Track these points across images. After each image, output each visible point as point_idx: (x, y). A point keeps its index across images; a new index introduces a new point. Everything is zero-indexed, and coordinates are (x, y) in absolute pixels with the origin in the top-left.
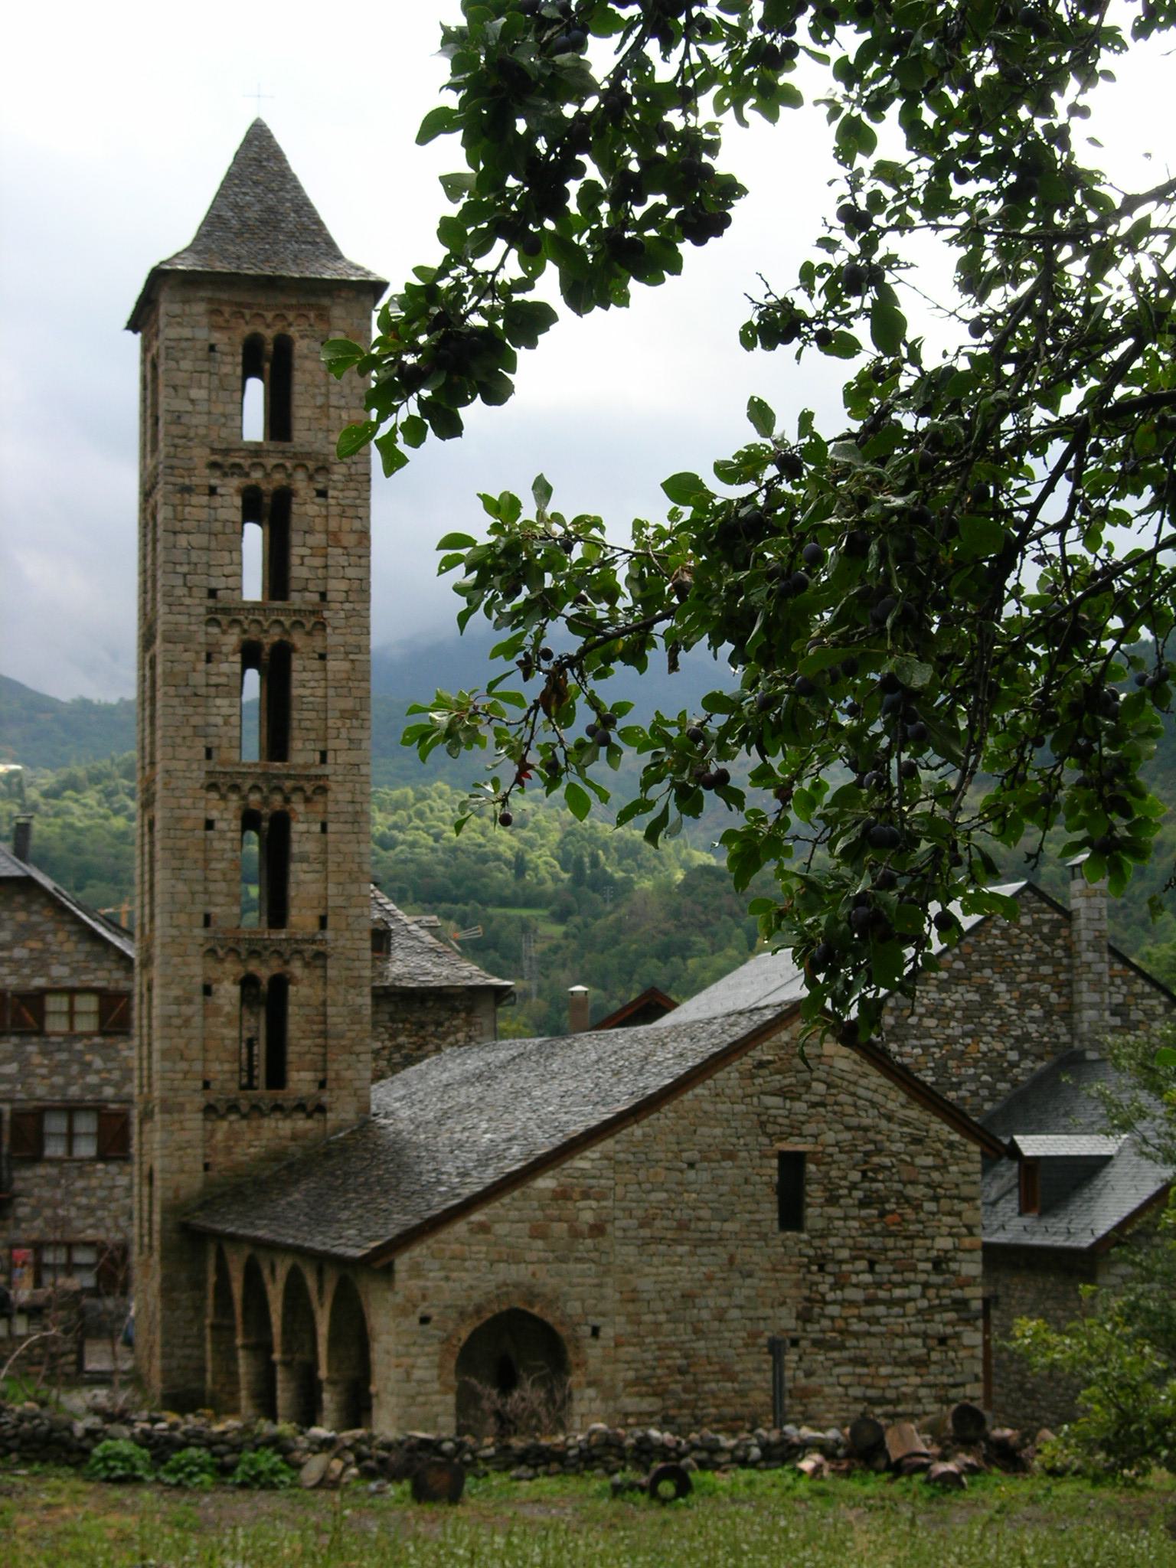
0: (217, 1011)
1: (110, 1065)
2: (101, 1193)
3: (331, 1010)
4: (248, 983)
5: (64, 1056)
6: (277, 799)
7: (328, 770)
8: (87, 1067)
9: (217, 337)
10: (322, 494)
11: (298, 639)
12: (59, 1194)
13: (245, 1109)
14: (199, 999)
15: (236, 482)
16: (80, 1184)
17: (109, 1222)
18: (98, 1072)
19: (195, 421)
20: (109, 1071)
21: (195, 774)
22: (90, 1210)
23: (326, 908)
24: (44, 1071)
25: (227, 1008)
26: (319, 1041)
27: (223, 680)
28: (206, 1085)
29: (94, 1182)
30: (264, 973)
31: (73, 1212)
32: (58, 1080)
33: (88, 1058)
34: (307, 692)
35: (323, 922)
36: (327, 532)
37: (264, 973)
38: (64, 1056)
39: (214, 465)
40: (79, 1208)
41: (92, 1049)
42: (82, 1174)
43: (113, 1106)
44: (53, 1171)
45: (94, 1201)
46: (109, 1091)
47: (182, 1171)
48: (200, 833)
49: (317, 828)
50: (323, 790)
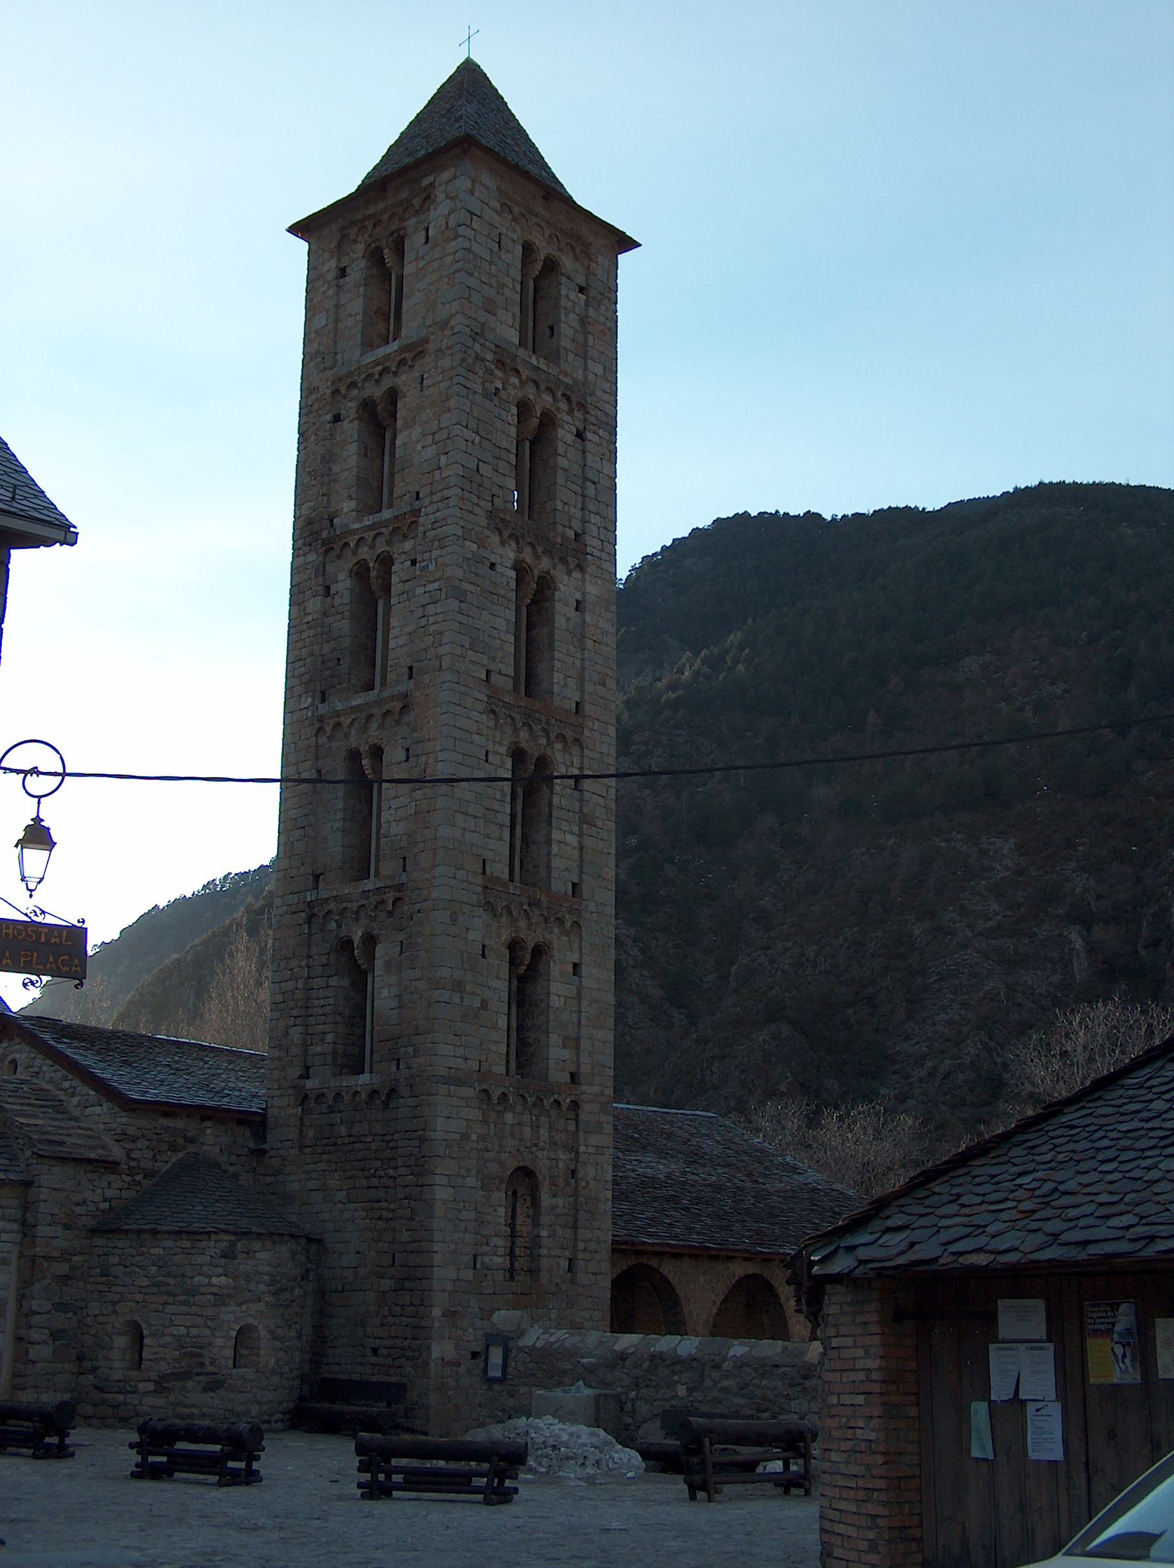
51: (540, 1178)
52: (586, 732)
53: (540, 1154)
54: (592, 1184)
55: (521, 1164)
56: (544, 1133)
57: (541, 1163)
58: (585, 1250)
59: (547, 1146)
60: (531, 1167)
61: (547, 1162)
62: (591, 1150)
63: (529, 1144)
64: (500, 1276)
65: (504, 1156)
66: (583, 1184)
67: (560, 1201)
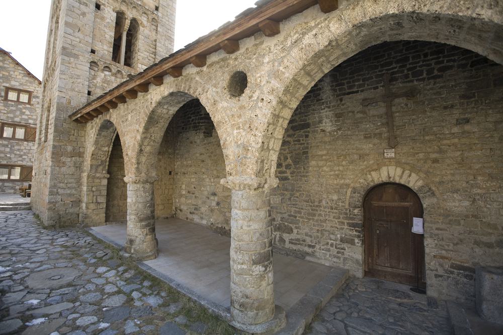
0: (103, 18)
1: (32, 114)
2: (25, 151)
3: (158, 44)
5: (14, 108)
8: (23, 113)
12: (8, 150)
13: (114, 71)
16: (16, 147)
17: (27, 160)
18: (27, 115)
20: (32, 116)
22: (21, 156)
24: (5, 112)
25: (108, 20)
26: (153, 56)
28: (93, 52)
29: (22, 148)
31: (13, 156)
32: (11, 115)
33: (24, 110)
35: (157, 8)
38: (14, 108)
40: (16, 154)
41: (25, 108)
42: (18, 144)
43: (31, 126)
44: (5, 142)
45: (22, 153)
46: (31, 121)
47: (73, 90)
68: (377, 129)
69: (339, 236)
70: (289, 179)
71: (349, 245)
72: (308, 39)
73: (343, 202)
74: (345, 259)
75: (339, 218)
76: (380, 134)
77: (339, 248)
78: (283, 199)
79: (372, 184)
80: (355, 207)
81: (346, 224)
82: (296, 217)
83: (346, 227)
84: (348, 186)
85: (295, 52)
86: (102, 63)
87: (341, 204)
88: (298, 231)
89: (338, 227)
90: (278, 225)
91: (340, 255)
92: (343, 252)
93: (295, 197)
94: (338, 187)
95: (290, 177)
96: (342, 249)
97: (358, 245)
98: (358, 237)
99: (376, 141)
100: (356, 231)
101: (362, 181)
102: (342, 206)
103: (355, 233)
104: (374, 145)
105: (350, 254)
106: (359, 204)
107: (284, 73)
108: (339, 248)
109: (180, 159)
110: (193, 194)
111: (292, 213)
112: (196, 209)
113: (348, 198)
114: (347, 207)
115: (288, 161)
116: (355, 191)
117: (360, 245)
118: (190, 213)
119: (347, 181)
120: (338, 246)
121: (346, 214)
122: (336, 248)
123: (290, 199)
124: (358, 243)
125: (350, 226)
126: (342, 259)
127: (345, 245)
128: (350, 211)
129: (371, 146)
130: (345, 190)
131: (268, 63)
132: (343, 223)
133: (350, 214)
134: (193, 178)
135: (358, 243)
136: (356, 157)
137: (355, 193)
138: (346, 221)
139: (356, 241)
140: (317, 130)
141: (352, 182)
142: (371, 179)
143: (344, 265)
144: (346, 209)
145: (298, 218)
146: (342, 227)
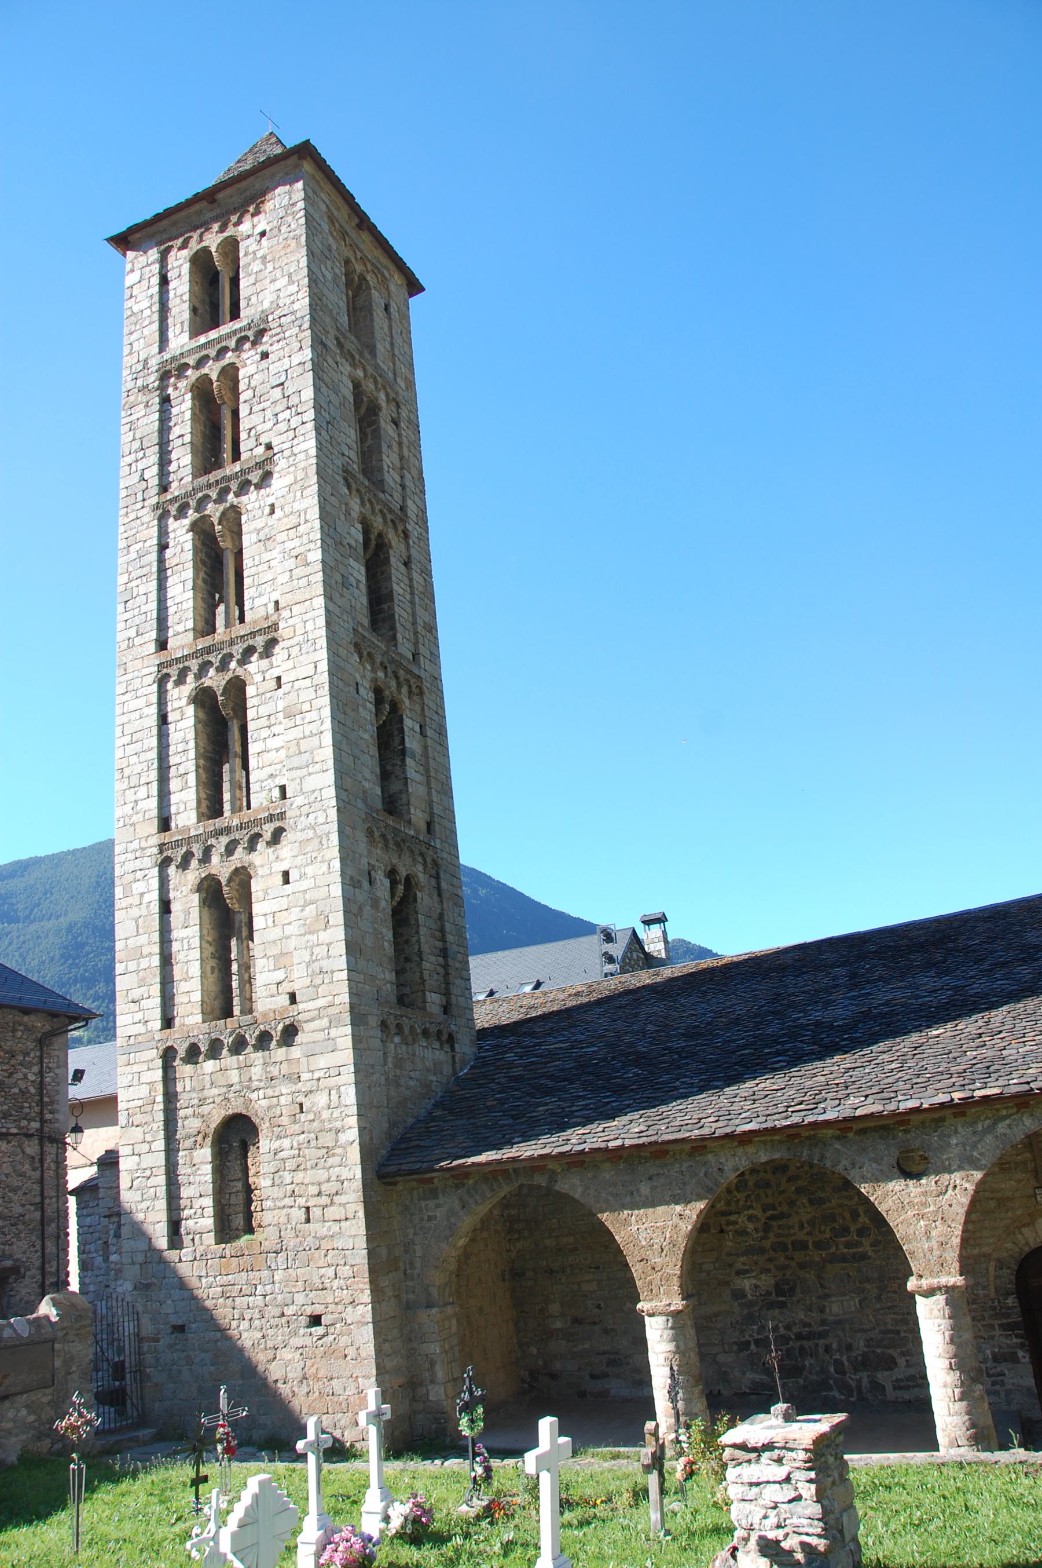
4: (392, 874)
6: (393, 683)
7: (423, 674)
9: (331, 240)
10: (396, 423)
11: (392, 536)
14: (366, 884)
15: (346, 368)
19: (326, 292)
21: (346, 625)
23: (432, 814)
27: (353, 544)
30: (403, 872)
34: (401, 591)
36: (401, 458)
37: (403, 872)
39: (337, 339)
48: (353, 690)
49: (417, 728)
50: (421, 693)
51: (256, 1121)
52: (281, 625)
53: (254, 1096)
54: (325, 1114)
55: (230, 1112)
56: (256, 1072)
57: (259, 1105)
58: (319, 1194)
59: (262, 1084)
60: (244, 1112)
61: (264, 1103)
62: (316, 1075)
63: (237, 1087)
64: (210, 1238)
65: (205, 1110)
66: (311, 1117)
67: (286, 1143)
68: (1017, 1155)
69: (988, 1352)
70: (869, 1258)
71: (1010, 1365)
72: (1002, 1128)
73: (984, 1288)
74: (1008, 1393)
75: (983, 1319)
76: (1025, 1163)
77: (993, 1375)
78: (864, 1299)
79: (1027, 1249)
80: (1007, 1294)
81: (997, 1327)
82: (898, 1332)
83: (998, 1332)
84: (987, 1256)
85: (989, 1139)
86: (392, 1017)
87: (981, 1292)
88: (907, 1361)
89: (985, 1335)
90: (860, 1358)
91: (997, 1387)
92: (1002, 1381)
93: (889, 1292)
94: (971, 1261)
95: (870, 1254)
96: (999, 1375)
97: (1024, 1360)
98: (1022, 1346)
99: (1019, 1175)
100: (1017, 1336)
101: (1009, 1245)
102: (986, 1296)
103: (1015, 1340)
104: (1018, 1181)
105: (1015, 1381)
106: (1012, 1287)
107: (979, 1160)
108: (993, 1375)
109: (526, 1233)
110: (595, 1323)
111: (890, 1327)
112: (612, 1363)
113: (991, 1279)
114: (992, 1296)
115: (861, 1220)
116: (1001, 1264)
117: (1027, 1360)
118: (593, 1377)
119: (986, 1249)
120: (991, 1372)
121: (994, 1308)
122: (988, 1375)
123: (879, 1298)
124: (1024, 1357)
125: (1005, 1330)
126: (1003, 1394)
127: (1002, 1367)
128: (999, 1302)
129: (1013, 1183)
130: (984, 1266)
131: (957, 1145)
132: (992, 1327)
133: (1002, 1308)
134: (588, 1281)
135: (1024, 1357)
136: (992, 1204)
137: (1001, 1269)
138: (996, 1322)
139: (1021, 1354)
140: (913, 1157)
141: (994, 1250)
142: (1023, 1242)
143: (1009, 1403)
144: (993, 1300)
145: (902, 1334)
146: (992, 1333)
